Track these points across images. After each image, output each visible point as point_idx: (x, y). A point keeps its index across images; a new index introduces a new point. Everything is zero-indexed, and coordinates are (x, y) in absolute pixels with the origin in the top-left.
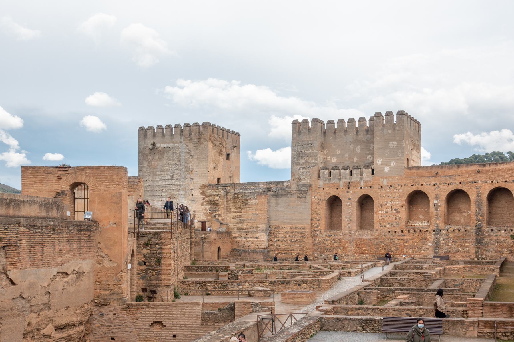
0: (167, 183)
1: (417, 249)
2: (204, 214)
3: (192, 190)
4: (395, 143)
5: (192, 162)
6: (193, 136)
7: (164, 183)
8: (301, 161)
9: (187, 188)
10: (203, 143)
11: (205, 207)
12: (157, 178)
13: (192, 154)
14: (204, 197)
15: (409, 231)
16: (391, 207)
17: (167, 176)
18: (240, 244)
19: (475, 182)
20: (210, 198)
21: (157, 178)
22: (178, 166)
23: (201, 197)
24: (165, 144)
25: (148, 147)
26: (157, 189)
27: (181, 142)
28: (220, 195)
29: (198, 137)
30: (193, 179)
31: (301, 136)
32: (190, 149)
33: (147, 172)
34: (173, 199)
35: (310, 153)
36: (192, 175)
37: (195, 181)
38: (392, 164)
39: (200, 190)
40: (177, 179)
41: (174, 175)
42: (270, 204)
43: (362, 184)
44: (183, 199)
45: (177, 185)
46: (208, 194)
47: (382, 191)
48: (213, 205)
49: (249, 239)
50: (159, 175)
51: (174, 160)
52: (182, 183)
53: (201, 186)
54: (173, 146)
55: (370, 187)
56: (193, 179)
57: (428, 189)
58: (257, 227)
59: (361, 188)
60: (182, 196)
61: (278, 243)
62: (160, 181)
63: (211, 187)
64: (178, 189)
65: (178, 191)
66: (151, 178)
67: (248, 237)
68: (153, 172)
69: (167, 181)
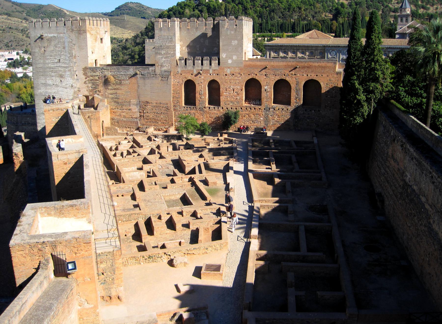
0: (55, 65)
1: (251, 122)
2: (87, 90)
3: (76, 71)
4: (236, 42)
6: (74, 28)
7: (53, 66)
8: (163, 52)
13: (73, 42)
15: (246, 109)
16: (233, 90)
17: (54, 59)
18: (117, 114)
19: (295, 75)
20: (91, 78)
21: (47, 62)
23: (84, 77)
26: (48, 70)
27: (64, 33)
31: (162, 32)
32: (72, 39)
35: (170, 45)
38: (234, 58)
39: (82, 71)
42: (139, 84)
43: (211, 72)
44: (70, 78)
45: (64, 67)
46: (89, 74)
47: (226, 78)
48: (93, 84)
49: (124, 110)
50: (48, 59)
51: (60, 47)
54: (59, 36)
55: (217, 74)
57: (261, 78)
58: (130, 102)
59: (210, 74)
60: (68, 76)
61: (147, 114)
66: (42, 61)
67: (123, 109)
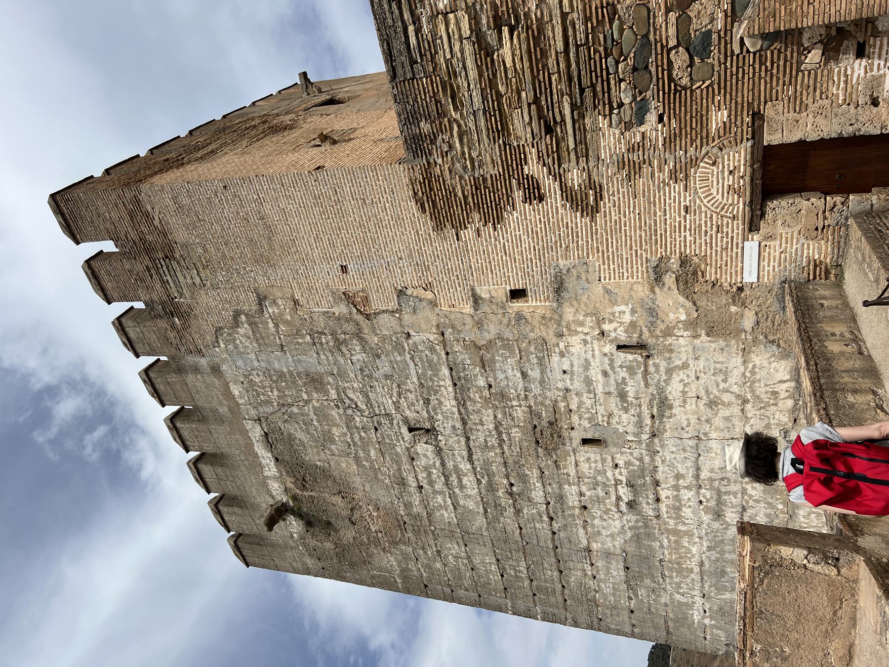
0: (465, 466)
3: (476, 300)
5: (296, 302)
7: (469, 480)
9: (470, 334)
10: (157, 222)
11: (606, 174)
12: (448, 515)
14: (518, 195)
22: (351, 396)
24: (256, 456)
25: (302, 538)
26: (508, 520)
27: (216, 370)
28: (475, 19)
29: (147, 262)
30: (401, 293)
32: (228, 315)
33: (423, 559)
34: (565, 434)
36: (376, 304)
37: (409, 278)
39: (468, 234)
40: (427, 402)
41: (406, 421)
45: (461, 403)
50: (425, 503)
52: (445, 371)
53: (439, 226)
54: (253, 413)
56: (401, 293)
60: (535, 374)
62: (462, 502)
63: (425, 126)
64: (487, 401)
65: (503, 396)
68: (417, 532)
69: (450, 464)
